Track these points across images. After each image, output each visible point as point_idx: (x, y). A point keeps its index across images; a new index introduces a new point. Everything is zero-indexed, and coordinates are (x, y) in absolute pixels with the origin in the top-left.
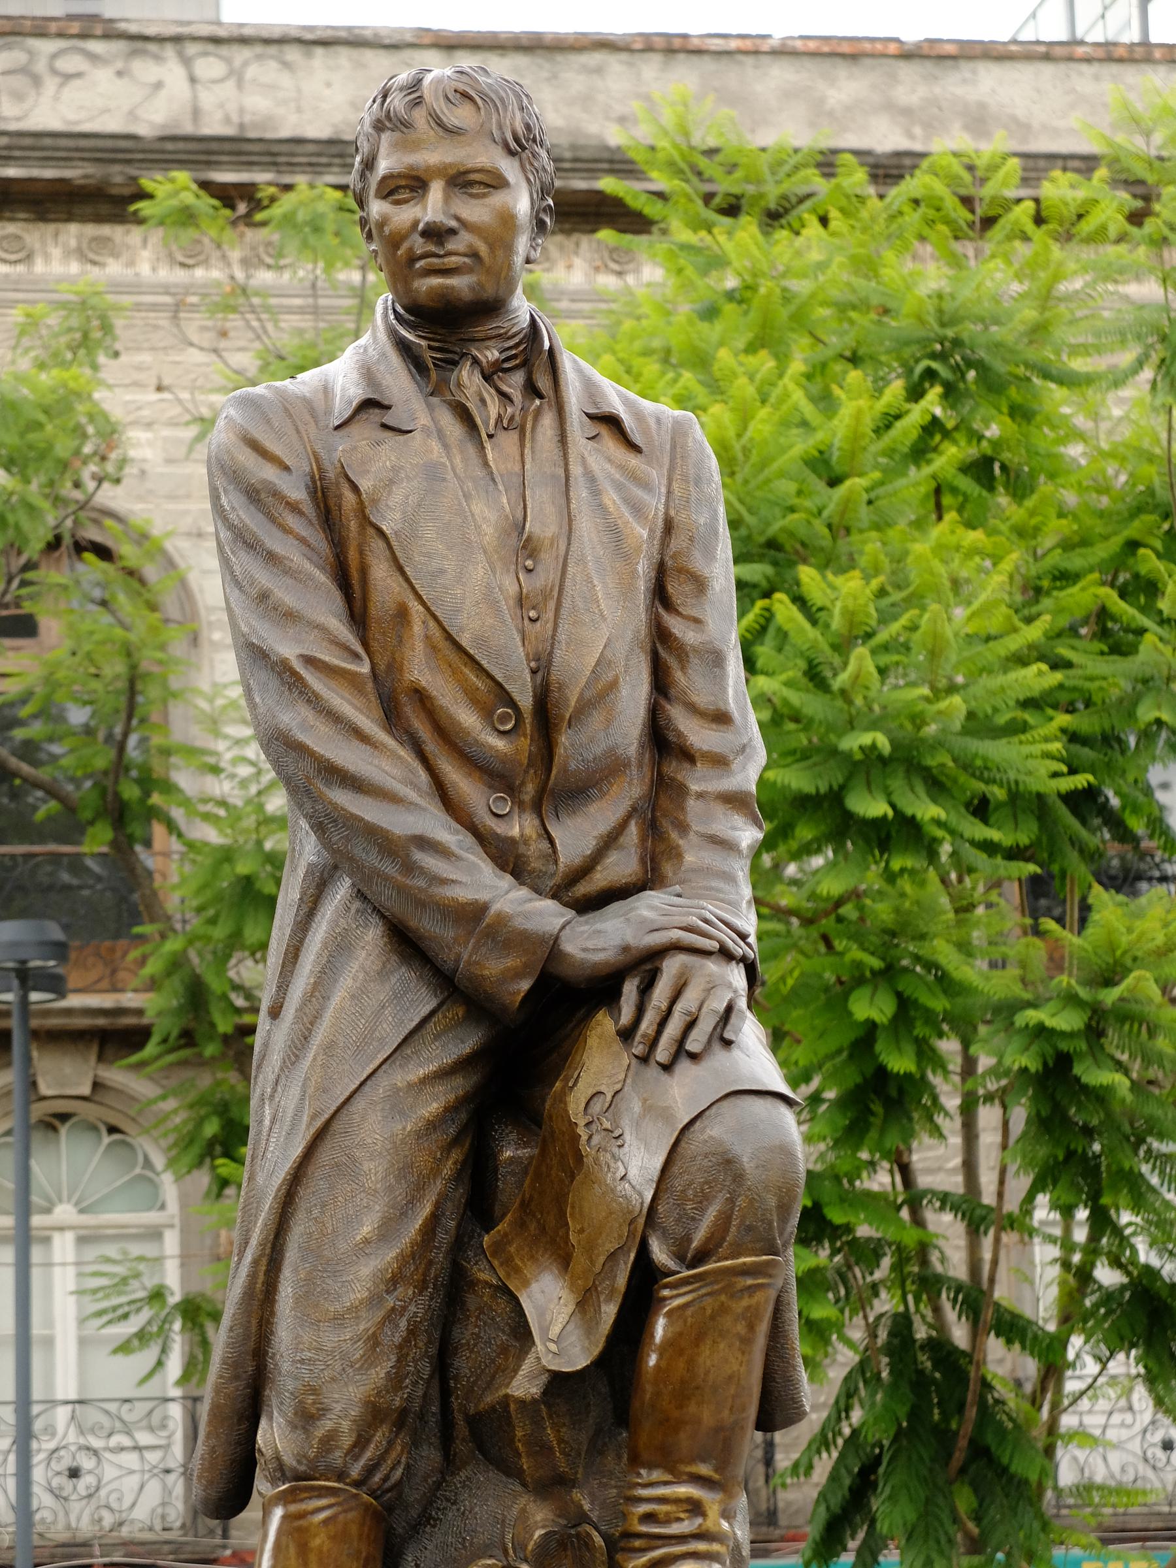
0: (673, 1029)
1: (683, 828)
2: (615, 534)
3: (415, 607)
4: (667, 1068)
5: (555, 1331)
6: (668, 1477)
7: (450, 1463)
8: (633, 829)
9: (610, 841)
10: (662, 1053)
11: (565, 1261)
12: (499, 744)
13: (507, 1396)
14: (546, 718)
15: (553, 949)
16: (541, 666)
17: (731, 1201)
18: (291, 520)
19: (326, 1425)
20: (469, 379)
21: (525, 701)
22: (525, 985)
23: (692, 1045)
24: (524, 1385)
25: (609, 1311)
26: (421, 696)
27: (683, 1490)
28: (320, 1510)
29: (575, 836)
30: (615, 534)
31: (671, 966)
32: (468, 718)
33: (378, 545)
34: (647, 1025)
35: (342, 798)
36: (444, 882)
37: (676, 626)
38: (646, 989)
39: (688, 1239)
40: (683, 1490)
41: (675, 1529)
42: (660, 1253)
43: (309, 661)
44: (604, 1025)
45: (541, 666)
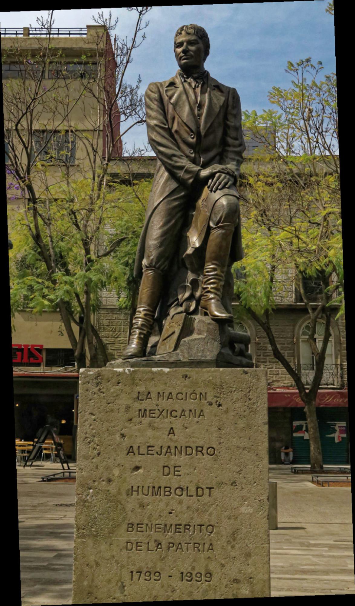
4: (215, 192)
7: (179, 268)
24: (190, 251)
25: (203, 236)
32: (185, 135)
42: (211, 224)
43: (156, 125)
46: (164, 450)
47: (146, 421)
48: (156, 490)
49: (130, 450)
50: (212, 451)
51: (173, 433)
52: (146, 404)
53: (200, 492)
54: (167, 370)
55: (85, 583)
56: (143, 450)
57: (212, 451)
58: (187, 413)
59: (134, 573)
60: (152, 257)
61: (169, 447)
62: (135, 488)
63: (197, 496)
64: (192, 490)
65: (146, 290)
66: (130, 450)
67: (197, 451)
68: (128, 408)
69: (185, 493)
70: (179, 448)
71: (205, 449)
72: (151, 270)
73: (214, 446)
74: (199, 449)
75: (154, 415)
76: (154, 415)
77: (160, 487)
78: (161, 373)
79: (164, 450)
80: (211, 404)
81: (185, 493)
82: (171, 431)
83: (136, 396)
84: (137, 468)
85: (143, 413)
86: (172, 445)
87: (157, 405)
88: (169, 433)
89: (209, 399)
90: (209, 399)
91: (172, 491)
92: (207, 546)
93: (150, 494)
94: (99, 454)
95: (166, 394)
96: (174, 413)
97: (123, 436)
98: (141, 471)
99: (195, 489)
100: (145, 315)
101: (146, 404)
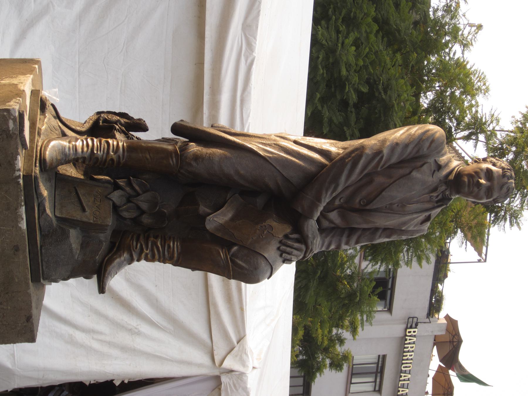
0: (288, 249)
1: (333, 237)
2: (404, 223)
3: (392, 180)
4: (278, 249)
5: (215, 219)
6: (179, 251)
8: (333, 226)
9: (331, 221)
10: (283, 248)
11: (232, 219)
12: (357, 201)
13: (199, 205)
16: (377, 210)
17: (246, 269)
18: (415, 151)
20: (443, 188)
21: (368, 207)
22: (300, 210)
23: (284, 255)
24: (203, 209)
26: (371, 182)
27: (176, 255)
28: (173, 161)
29: (334, 216)
30: (404, 223)
31: (303, 247)
32: (364, 193)
33: (407, 171)
34: (290, 242)
35: (348, 167)
37: (380, 231)
38: (298, 241)
39: (237, 258)
40: (176, 255)
41: (166, 253)
43: (382, 157)
45: (377, 210)
54: (23, 225)
60: (194, 164)
65: (148, 156)
72: (177, 162)
78: (17, 218)
100: (112, 160)
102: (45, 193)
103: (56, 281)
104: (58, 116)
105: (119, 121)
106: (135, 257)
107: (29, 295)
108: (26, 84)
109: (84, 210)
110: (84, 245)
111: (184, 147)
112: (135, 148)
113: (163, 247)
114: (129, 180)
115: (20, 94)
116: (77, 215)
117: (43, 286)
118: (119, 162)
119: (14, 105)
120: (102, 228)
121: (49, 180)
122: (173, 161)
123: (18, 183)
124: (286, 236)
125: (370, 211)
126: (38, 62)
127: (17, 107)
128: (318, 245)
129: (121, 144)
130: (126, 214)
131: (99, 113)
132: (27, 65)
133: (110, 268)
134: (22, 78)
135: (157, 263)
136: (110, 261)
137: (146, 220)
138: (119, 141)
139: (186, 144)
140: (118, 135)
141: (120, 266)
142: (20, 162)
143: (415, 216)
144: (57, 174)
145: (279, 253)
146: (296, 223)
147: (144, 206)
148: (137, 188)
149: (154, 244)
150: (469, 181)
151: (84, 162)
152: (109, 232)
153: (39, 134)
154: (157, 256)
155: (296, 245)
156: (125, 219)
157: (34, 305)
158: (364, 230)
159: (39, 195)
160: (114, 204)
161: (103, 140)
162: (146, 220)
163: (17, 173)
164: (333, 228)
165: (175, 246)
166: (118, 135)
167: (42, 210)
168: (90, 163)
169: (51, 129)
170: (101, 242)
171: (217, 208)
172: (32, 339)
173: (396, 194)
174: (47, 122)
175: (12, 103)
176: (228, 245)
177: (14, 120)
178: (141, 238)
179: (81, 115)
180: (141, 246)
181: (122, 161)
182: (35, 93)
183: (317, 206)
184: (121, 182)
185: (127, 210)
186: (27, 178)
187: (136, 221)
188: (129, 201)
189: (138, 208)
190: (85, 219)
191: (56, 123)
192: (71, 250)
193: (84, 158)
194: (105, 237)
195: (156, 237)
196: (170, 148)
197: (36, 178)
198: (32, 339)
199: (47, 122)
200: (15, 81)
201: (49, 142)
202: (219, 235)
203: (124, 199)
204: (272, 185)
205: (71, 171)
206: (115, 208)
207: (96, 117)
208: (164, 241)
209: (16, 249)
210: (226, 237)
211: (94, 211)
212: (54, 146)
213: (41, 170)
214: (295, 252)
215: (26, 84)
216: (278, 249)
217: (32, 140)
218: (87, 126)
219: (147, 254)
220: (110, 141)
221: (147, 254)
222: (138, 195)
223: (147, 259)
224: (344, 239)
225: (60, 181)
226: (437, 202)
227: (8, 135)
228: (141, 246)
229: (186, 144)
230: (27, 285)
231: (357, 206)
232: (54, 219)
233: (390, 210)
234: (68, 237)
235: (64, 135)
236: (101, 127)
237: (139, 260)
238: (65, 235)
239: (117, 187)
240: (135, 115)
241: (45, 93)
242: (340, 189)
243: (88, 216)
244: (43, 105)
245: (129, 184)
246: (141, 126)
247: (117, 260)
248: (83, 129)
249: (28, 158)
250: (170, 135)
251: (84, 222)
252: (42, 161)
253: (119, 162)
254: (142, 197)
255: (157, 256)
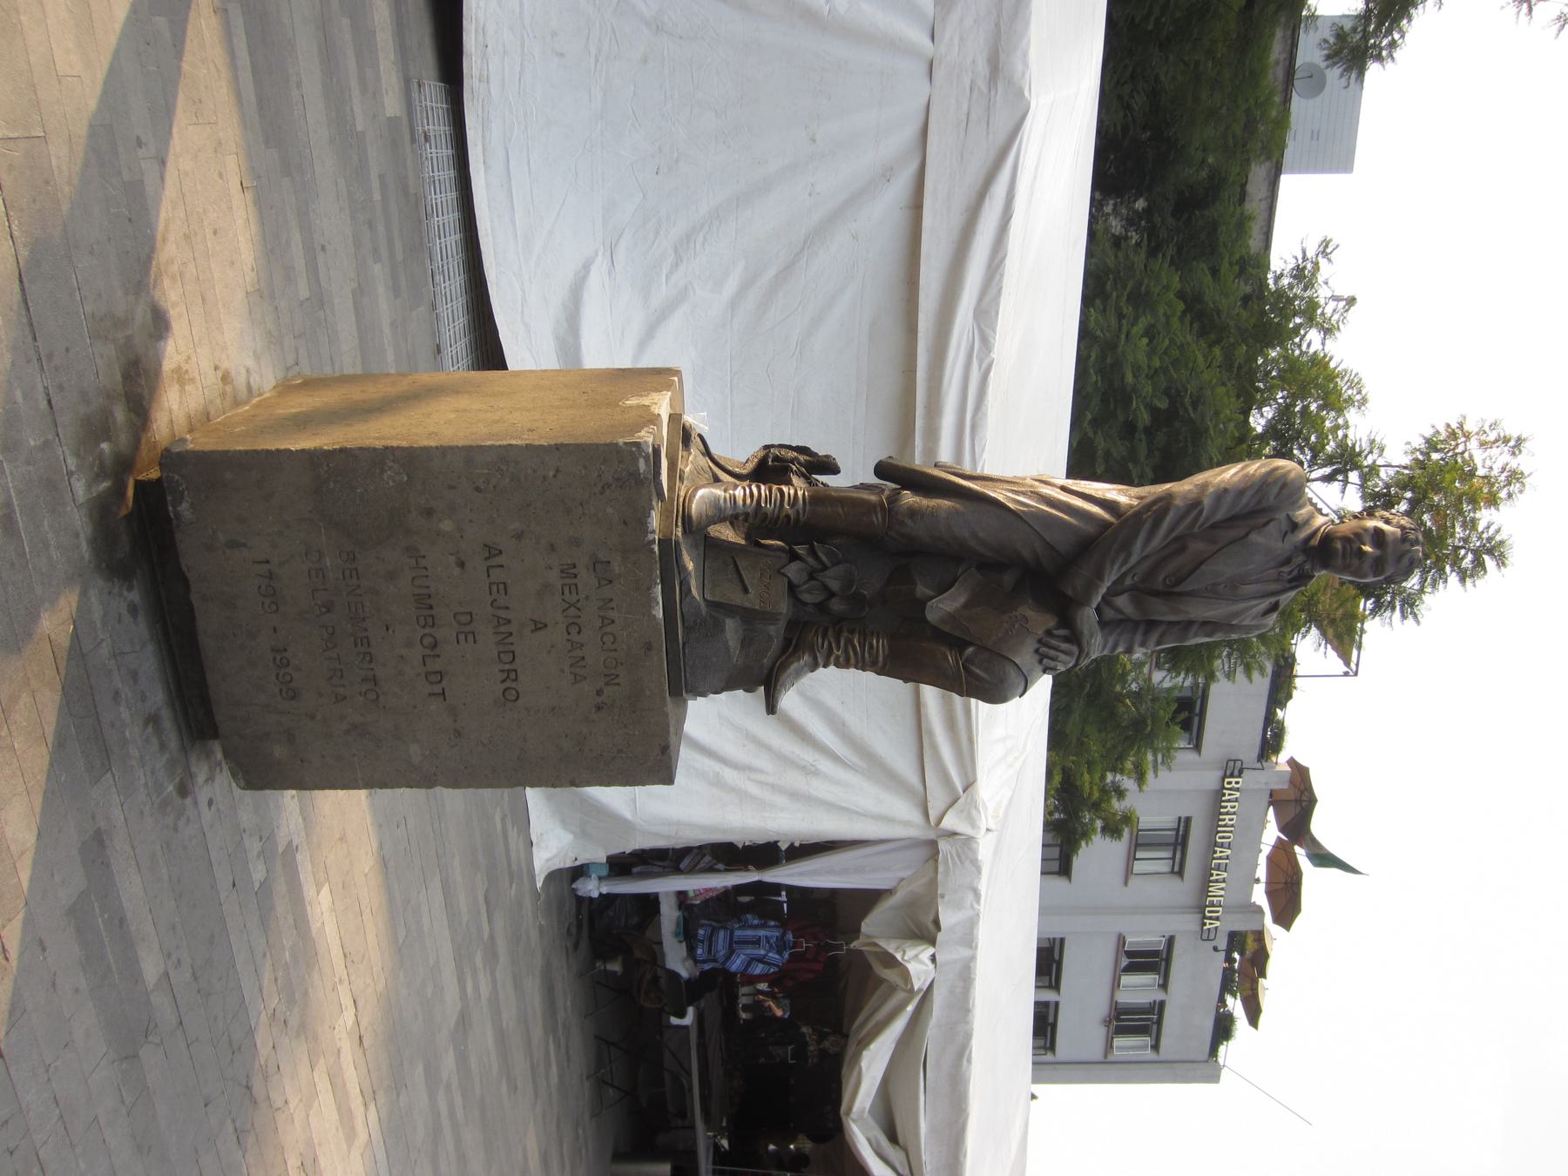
0: (1052, 652)
4: (1037, 651)
9: (1118, 610)
11: (966, 606)
14: (1167, 594)
15: (1085, 602)
16: (1190, 594)
19: (909, 522)
20: (1301, 559)
21: (1177, 589)
22: (1070, 592)
24: (921, 590)
26: (1183, 549)
29: (1122, 601)
30: (1236, 615)
31: (1075, 649)
32: (1173, 565)
33: (1243, 533)
34: (1054, 642)
35: (1147, 526)
36: (1112, 565)
38: (1067, 639)
43: (1201, 512)
44: (1051, 622)
45: (1190, 594)
46: (502, 613)
47: (554, 577)
48: (425, 602)
49: (492, 551)
50: (510, 697)
51: (537, 629)
52: (586, 578)
53: (434, 678)
54: (659, 612)
55: (228, 476)
56: (497, 575)
57: (510, 697)
58: (578, 653)
59: (267, 567)
60: (909, 522)
61: (509, 621)
62: (423, 562)
63: (427, 674)
64: (436, 665)
66: (492, 551)
67: (509, 671)
68: (576, 542)
69: (428, 652)
70: (510, 640)
71: (514, 685)
73: (520, 701)
74: (511, 675)
75: (567, 591)
76: (567, 591)
77: (431, 607)
78: (650, 602)
79: (502, 613)
80: (599, 693)
81: (428, 652)
82: (539, 626)
83: (602, 556)
84: (462, 565)
85: (569, 572)
86: (513, 628)
87: (587, 598)
88: (535, 622)
89: (608, 691)
90: (608, 691)
91: (427, 631)
92: (341, 690)
93: (417, 591)
94: (478, 489)
95: (611, 614)
96: (574, 630)
97: (519, 536)
98: (457, 571)
99: (437, 668)
100: (788, 516)
101: (586, 578)
102: (690, 566)
103: (703, 695)
104: (707, 452)
105: (796, 458)
106: (820, 660)
107: (667, 715)
108: (662, 405)
109: (746, 591)
110: (745, 642)
111: (894, 498)
112: (821, 499)
113: (862, 646)
114: (812, 546)
115: (654, 420)
116: (737, 598)
117: (685, 702)
118: (797, 520)
119: (646, 436)
120: (772, 618)
121: (696, 546)
122: (877, 519)
123: (652, 551)
124: (1049, 633)
125: (1181, 594)
126: (677, 373)
127: (650, 440)
128: (1097, 646)
129: (800, 493)
130: (806, 597)
131: (767, 447)
132: (662, 377)
133: (783, 678)
134: (655, 396)
135: (852, 670)
136: (784, 667)
137: (836, 606)
138: (797, 488)
139: (896, 493)
140: (795, 480)
141: (799, 674)
142: (655, 520)
143: (1254, 602)
144: (707, 537)
145: (1037, 657)
146: (1065, 612)
147: (835, 585)
148: (824, 558)
149: (849, 642)
150: (1344, 547)
151: (746, 520)
152: (782, 624)
153: (681, 479)
154: (853, 661)
155: (1064, 646)
156: (806, 604)
157: (672, 729)
158: (1170, 623)
159: (682, 568)
160: (790, 582)
161: (775, 487)
162: (836, 606)
163: (650, 537)
164: (1121, 621)
165: (880, 645)
166: (795, 480)
167: (685, 591)
168: (756, 523)
169: (698, 471)
170: (770, 638)
171: (942, 589)
172: (669, 780)
173: (1223, 568)
174: (692, 461)
175: (643, 433)
176: (959, 644)
177: (647, 458)
178: (830, 633)
179: (741, 451)
180: (830, 644)
181: (802, 519)
182: (675, 418)
183: (1097, 587)
184: (801, 550)
185: (809, 591)
186: (665, 543)
187: (821, 607)
188: (811, 577)
189: (825, 587)
190: (747, 605)
191: (704, 462)
192: (727, 648)
193: (747, 514)
194: (776, 631)
195: (852, 632)
196: (873, 498)
197: (677, 543)
198: (669, 780)
199: (692, 461)
200: (646, 401)
201: (696, 490)
202: (946, 629)
203: (805, 576)
204: (1026, 553)
205: (726, 533)
206: (792, 588)
207: (762, 454)
208: (864, 637)
209: (649, 647)
210: (957, 633)
211: (764, 592)
212: (704, 496)
213: (684, 532)
214: (1062, 657)
215: (662, 405)
216: (1037, 651)
217: (671, 487)
218: (750, 466)
219: (838, 657)
220: (785, 489)
221: (838, 657)
222: (825, 568)
223: (838, 665)
224: (1138, 638)
225: (711, 548)
226: (1290, 581)
227: (636, 480)
228: (830, 644)
229: (896, 493)
230: (664, 699)
231: (1160, 587)
232: (703, 604)
233: (1213, 593)
234: (723, 630)
235: (717, 480)
236: (770, 468)
237: (825, 666)
238: (719, 628)
239: (794, 557)
240: (821, 450)
241: (688, 419)
242: (1133, 560)
243: (752, 600)
244: (686, 436)
245: (813, 552)
246: (829, 467)
247: (795, 665)
248: (744, 472)
249: (666, 514)
250: (873, 480)
251: (745, 609)
252: (687, 519)
253: (797, 520)
254: (832, 572)
255: (853, 661)
